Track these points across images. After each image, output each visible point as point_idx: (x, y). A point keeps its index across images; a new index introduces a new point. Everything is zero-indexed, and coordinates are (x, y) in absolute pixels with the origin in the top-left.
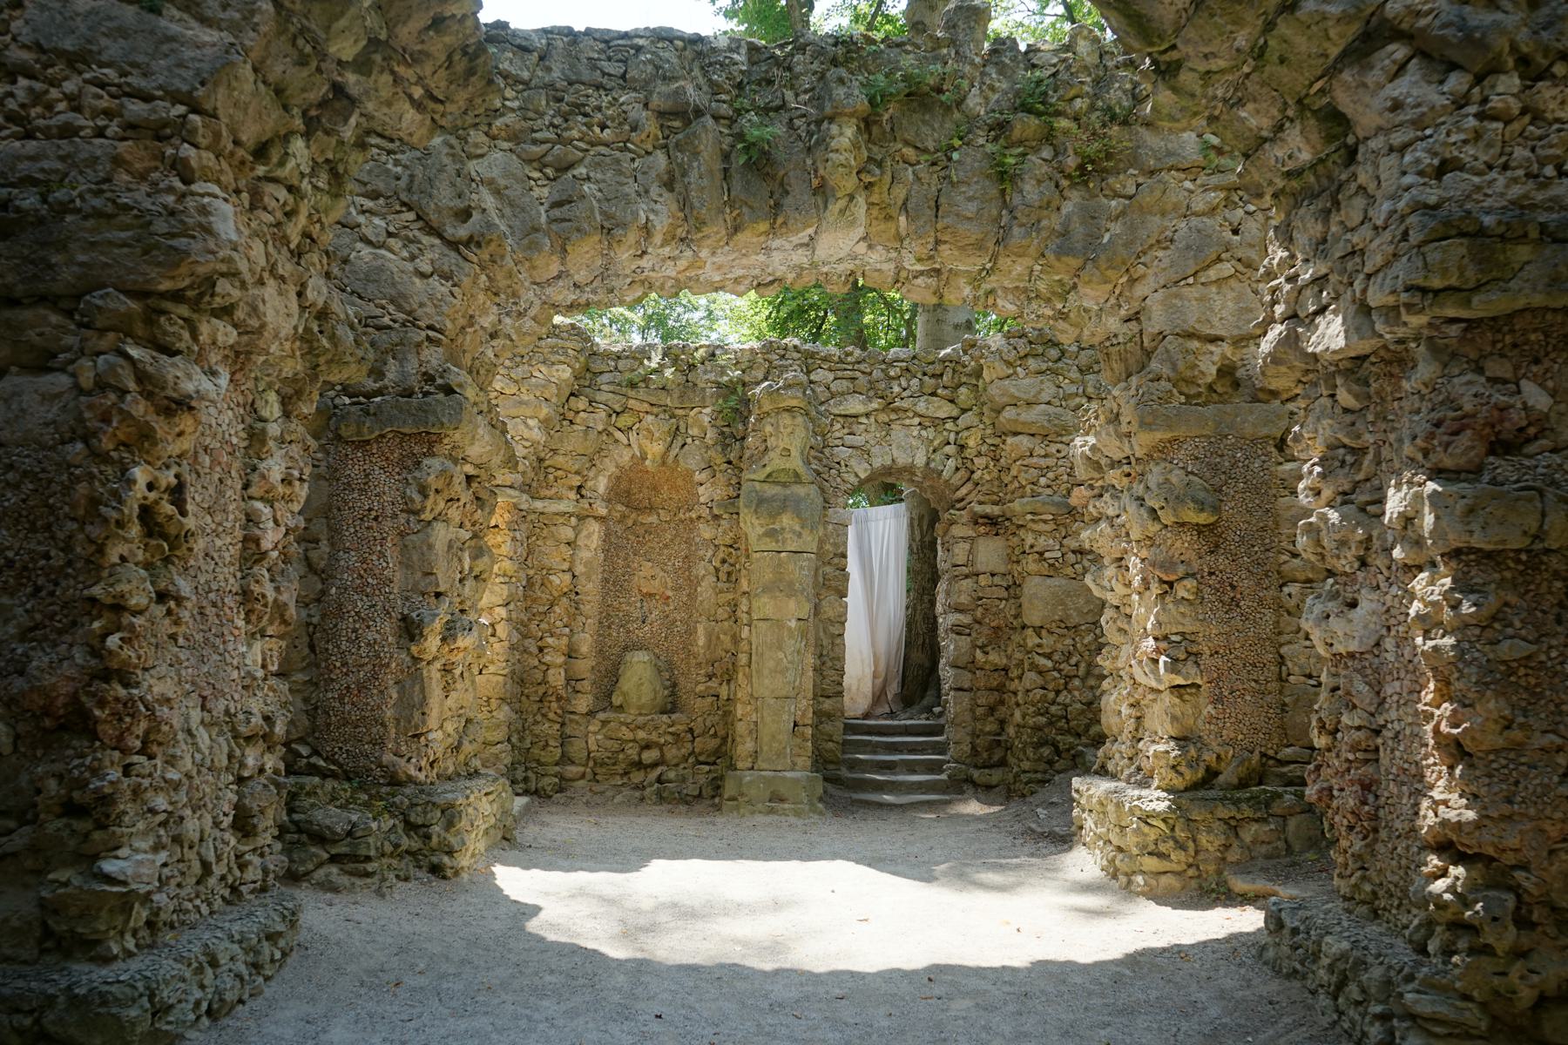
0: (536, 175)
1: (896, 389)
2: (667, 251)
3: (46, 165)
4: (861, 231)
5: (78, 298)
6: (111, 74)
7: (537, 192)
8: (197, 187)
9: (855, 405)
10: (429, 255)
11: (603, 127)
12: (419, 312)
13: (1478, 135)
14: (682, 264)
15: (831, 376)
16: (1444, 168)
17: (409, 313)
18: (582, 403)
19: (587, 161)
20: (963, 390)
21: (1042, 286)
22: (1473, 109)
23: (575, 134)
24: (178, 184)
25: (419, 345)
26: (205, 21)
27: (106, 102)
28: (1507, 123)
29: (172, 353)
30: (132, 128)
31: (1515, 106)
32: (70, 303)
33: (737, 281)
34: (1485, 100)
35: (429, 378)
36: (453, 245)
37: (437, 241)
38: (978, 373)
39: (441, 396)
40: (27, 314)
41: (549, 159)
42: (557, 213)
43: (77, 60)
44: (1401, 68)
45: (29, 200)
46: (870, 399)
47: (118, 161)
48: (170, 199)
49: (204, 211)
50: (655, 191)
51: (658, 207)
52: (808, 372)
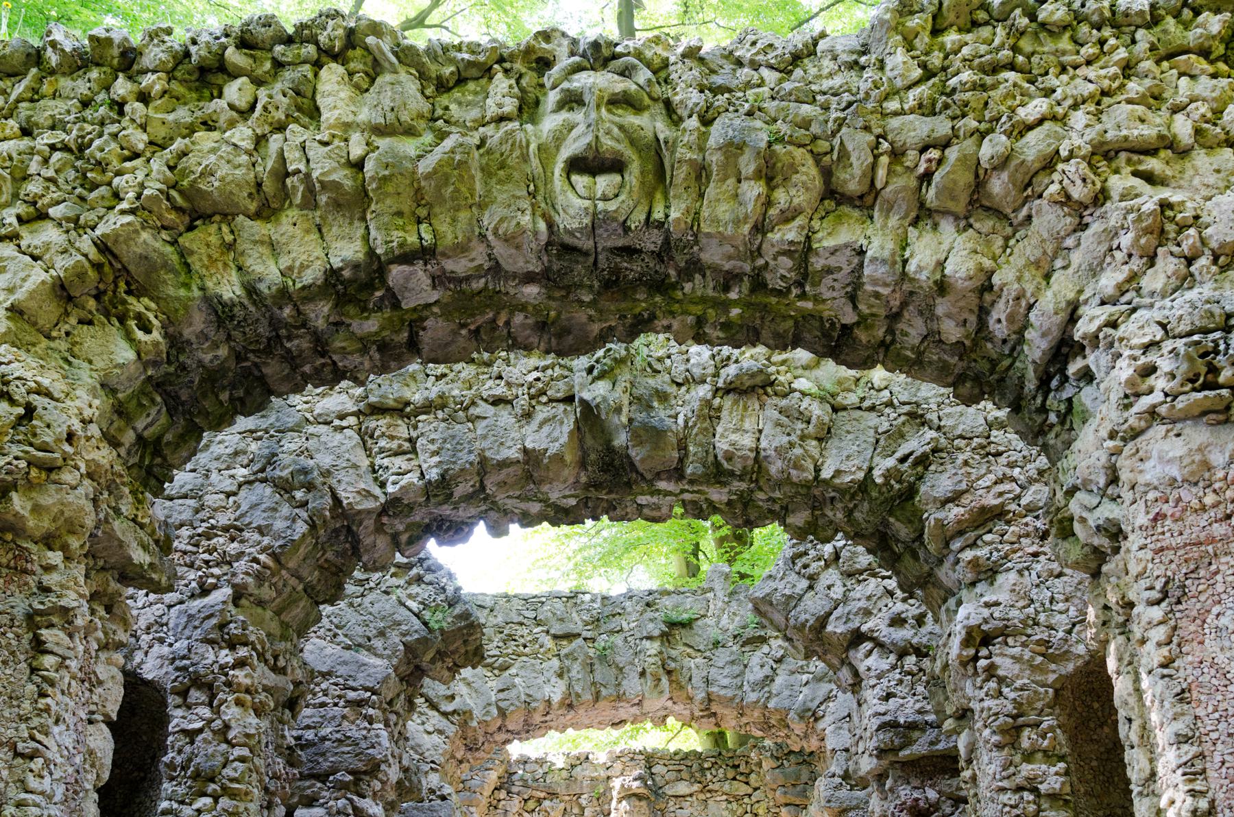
0: (489, 674)
1: (709, 777)
2: (560, 712)
3: (315, 720)
4: (667, 695)
5: (328, 776)
6: (341, 681)
7: (490, 684)
8: (375, 726)
9: (682, 788)
10: (433, 721)
11: (525, 646)
12: (427, 754)
13: (900, 682)
14: (568, 717)
15: (666, 769)
16: (888, 696)
17: (421, 754)
18: (503, 795)
19: (517, 665)
20: (753, 776)
21: (773, 722)
22: (898, 671)
23: (510, 651)
24: (366, 724)
25: (427, 773)
26: (376, 655)
27: (337, 693)
28: (913, 676)
29: (364, 797)
30: (349, 703)
31: (915, 669)
32: (323, 777)
33: (600, 723)
34: (903, 667)
35: (432, 791)
36: (445, 714)
37: (436, 714)
38: (760, 765)
39: (439, 802)
40: (307, 783)
41: (496, 665)
42: (501, 696)
43: (326, 675)
44: (870, 653)
45: (309, 735)
46: (692, 784)
47: (344, 717)
48: (364, 732)
49: (377, 736)
50: (553, 679)
51: (555, 690)
52: (650, 768)
